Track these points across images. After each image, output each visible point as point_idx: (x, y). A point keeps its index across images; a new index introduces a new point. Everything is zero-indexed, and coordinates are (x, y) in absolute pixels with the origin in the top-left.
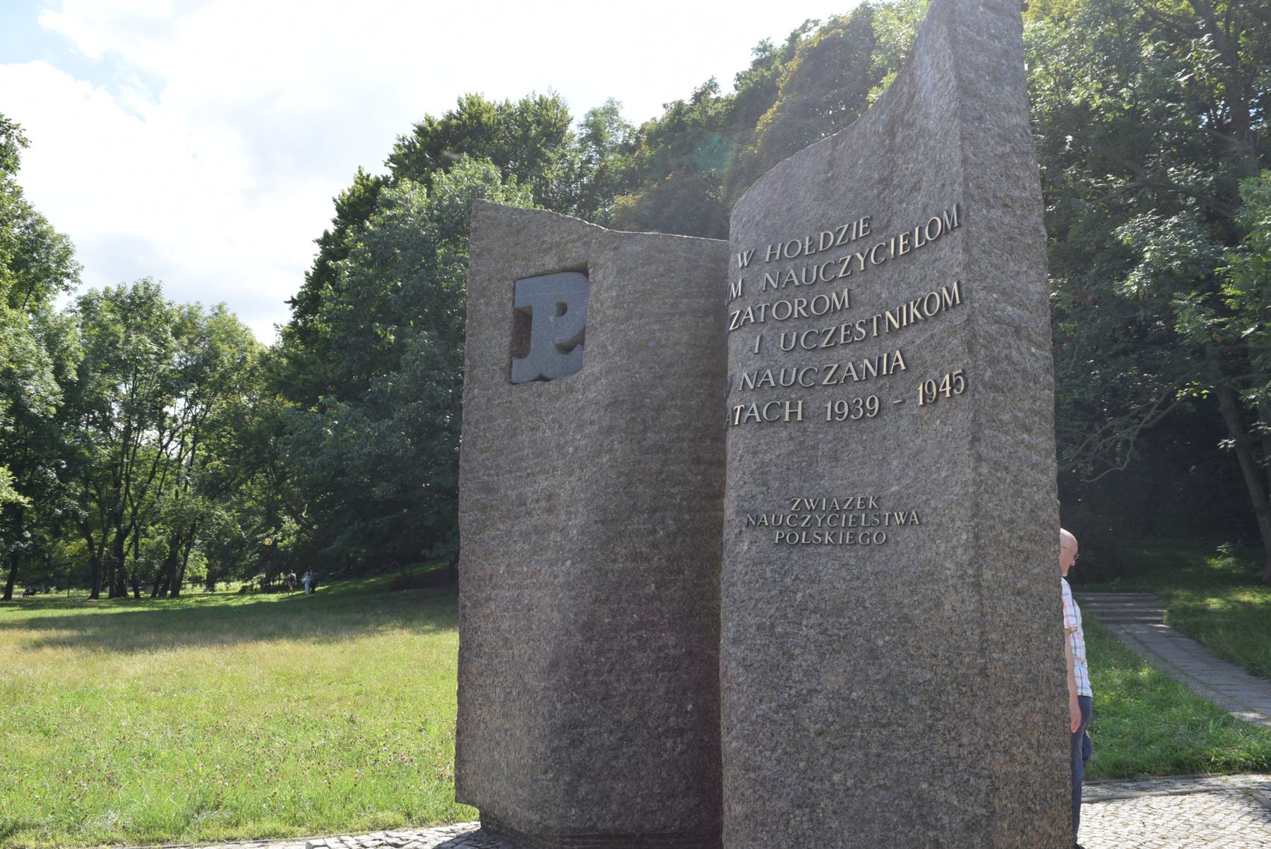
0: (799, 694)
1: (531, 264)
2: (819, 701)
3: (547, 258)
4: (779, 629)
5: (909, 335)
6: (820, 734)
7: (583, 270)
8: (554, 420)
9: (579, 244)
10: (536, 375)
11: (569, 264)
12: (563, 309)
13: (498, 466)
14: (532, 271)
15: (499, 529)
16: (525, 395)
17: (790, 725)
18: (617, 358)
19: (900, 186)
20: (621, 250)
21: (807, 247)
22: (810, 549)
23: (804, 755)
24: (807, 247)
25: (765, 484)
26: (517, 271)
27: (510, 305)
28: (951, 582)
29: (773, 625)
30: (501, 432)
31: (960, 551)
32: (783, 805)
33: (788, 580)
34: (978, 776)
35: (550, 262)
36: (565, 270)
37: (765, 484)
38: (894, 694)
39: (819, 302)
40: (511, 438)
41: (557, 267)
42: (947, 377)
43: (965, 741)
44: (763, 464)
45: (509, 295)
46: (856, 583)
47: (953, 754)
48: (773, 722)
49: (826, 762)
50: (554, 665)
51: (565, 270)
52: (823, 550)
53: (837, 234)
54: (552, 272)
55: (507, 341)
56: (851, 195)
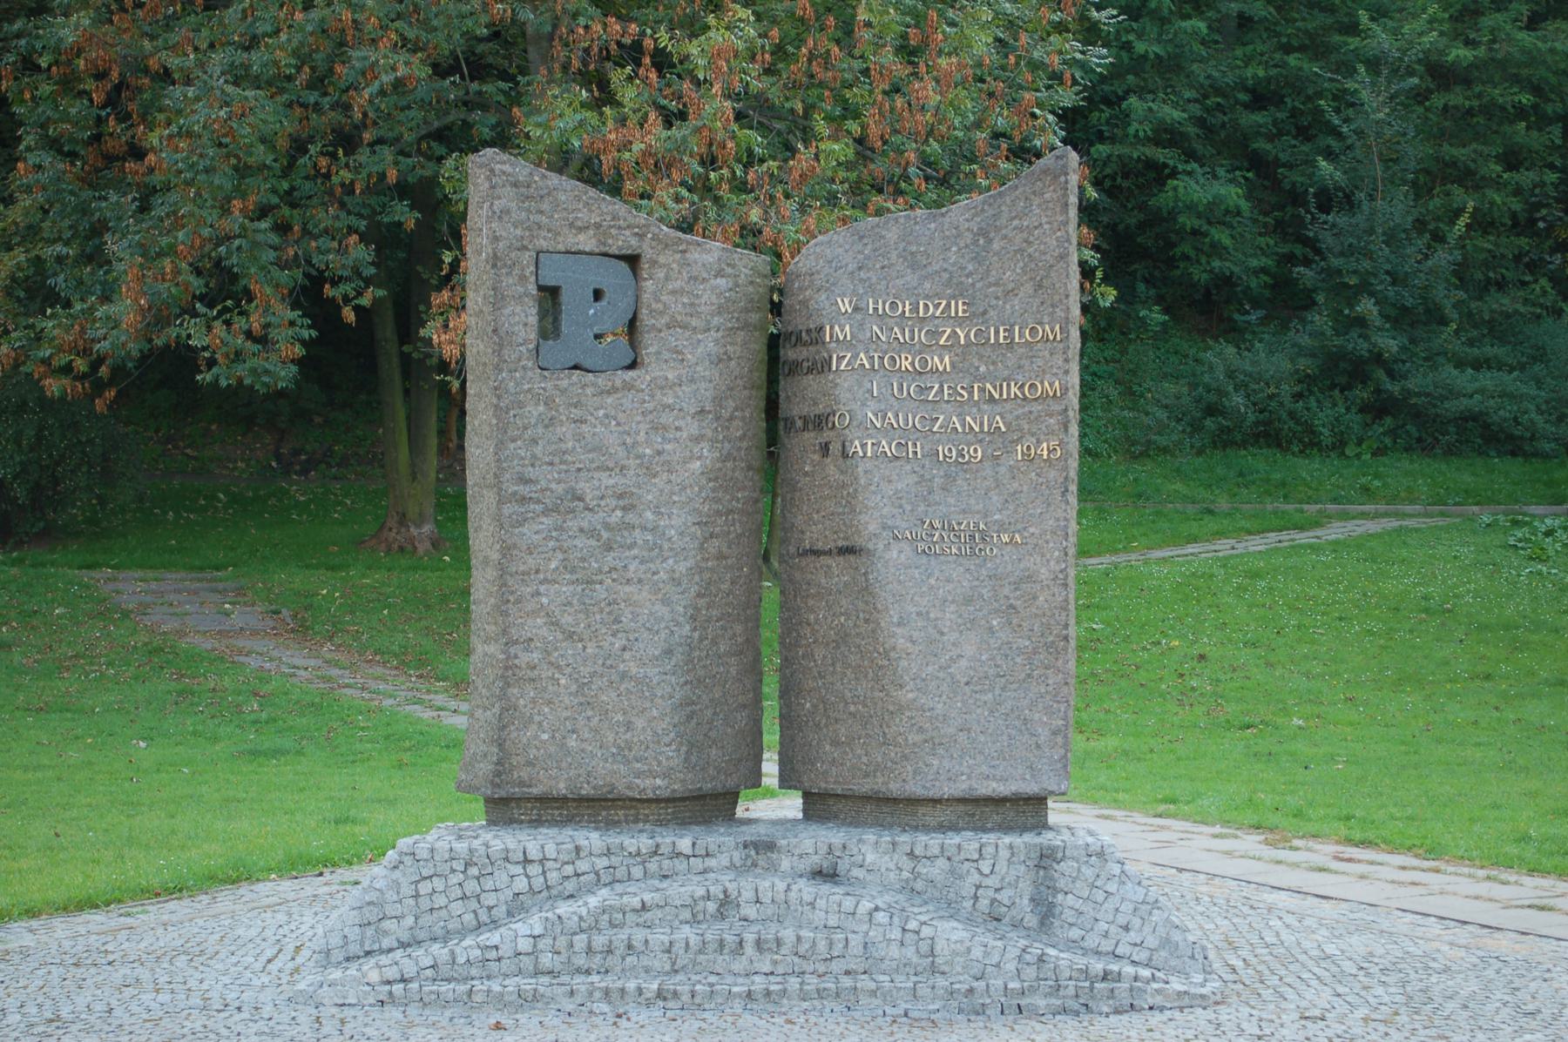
0: (951, 658)
1: (560, 239)
2: (964, 663)
3: (581, 237)
4: (932, 615)
5: (1008, 406)
6: (967, 684)
7: (633, 260)
8: (606, 416)
9: (627, 233)
10: (572, 364)
11: (614, 250)
12: (598, 295)
13: (534, 456)
14: (561, 247)
15: (543, 523)
16: (564, 383)
17: (949, 680)
18: (698, 369)
19: (997, 284)
20: (688, 255)
21: (907, 309)
22: (942, 558)
23: (959, 698)
24: (907, 309)
25: (901, 506)
26: (543, 244)
27: (534, 278)
28: (1045, 583)
29: (928, 613)
30: (533, 421)
31: (1052, 563)
32: (952, 730)
33: (932, 581)
34: (1058, 702)
35: (587, 242)
36: (606, 255)
37: (901, 506)
38: (1007, 656)
39: (924, 362)
40: (546, 427)
41: (597, 250)
42: (1045, 445)
43: (1050, 682)
44: (897, 491)
45: (532, 268)
46: (976, 583)
47: (1043, 690)
48: (937, 678)
49: (971, 701)
50: (669, 652)
51: (606, 255)
52: (950, 558)
53: (937, 306)
54: (587, 253)
55: (533, 320)
56: (946, 276)
